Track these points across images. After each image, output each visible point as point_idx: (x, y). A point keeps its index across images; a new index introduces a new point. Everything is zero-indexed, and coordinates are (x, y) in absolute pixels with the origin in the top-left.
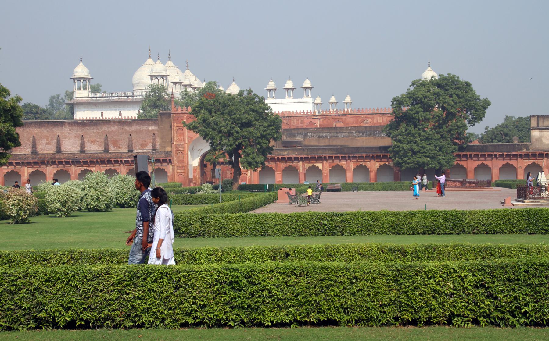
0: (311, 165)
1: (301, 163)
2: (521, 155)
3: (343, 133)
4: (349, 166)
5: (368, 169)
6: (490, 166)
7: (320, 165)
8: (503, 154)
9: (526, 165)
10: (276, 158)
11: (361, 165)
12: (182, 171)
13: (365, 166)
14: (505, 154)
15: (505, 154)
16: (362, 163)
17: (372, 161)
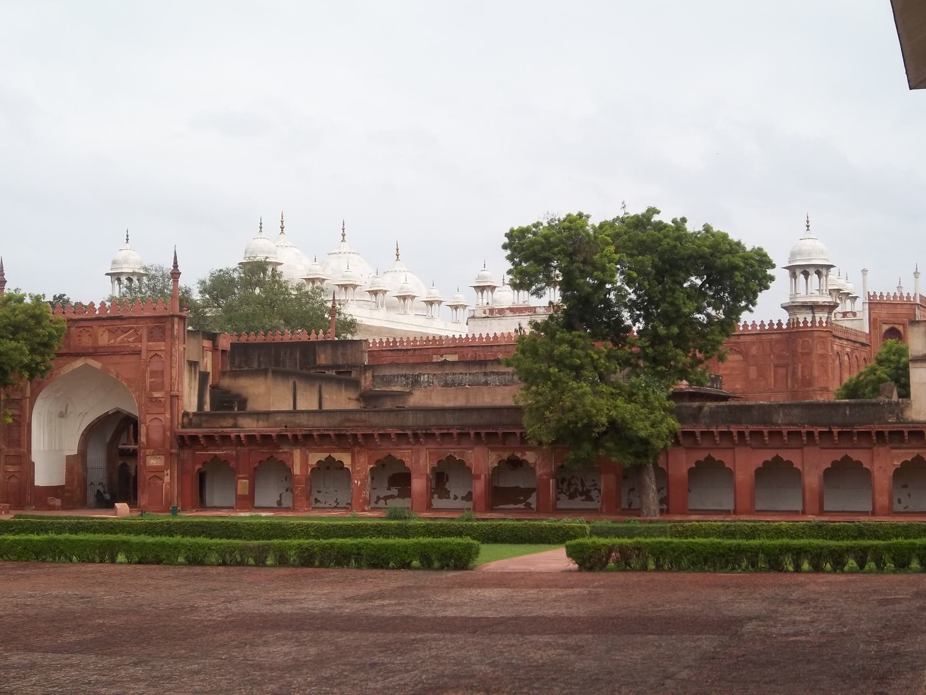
0: (322, 456)
1: (297, 454)
2: (880, 434)
3: (498, 374)
4: (417, 461)
5: (469, 469)
6: (797, 464)
7: (346, 459)
8: (830, 433)
9: (898, 463)
10: (233, 435)
11: (451, 458)
12: (16, 468)
13: (462, 463)
14: (836, 430)
15: (836, 430)
16: (451, 452)
17: (478, 449)
